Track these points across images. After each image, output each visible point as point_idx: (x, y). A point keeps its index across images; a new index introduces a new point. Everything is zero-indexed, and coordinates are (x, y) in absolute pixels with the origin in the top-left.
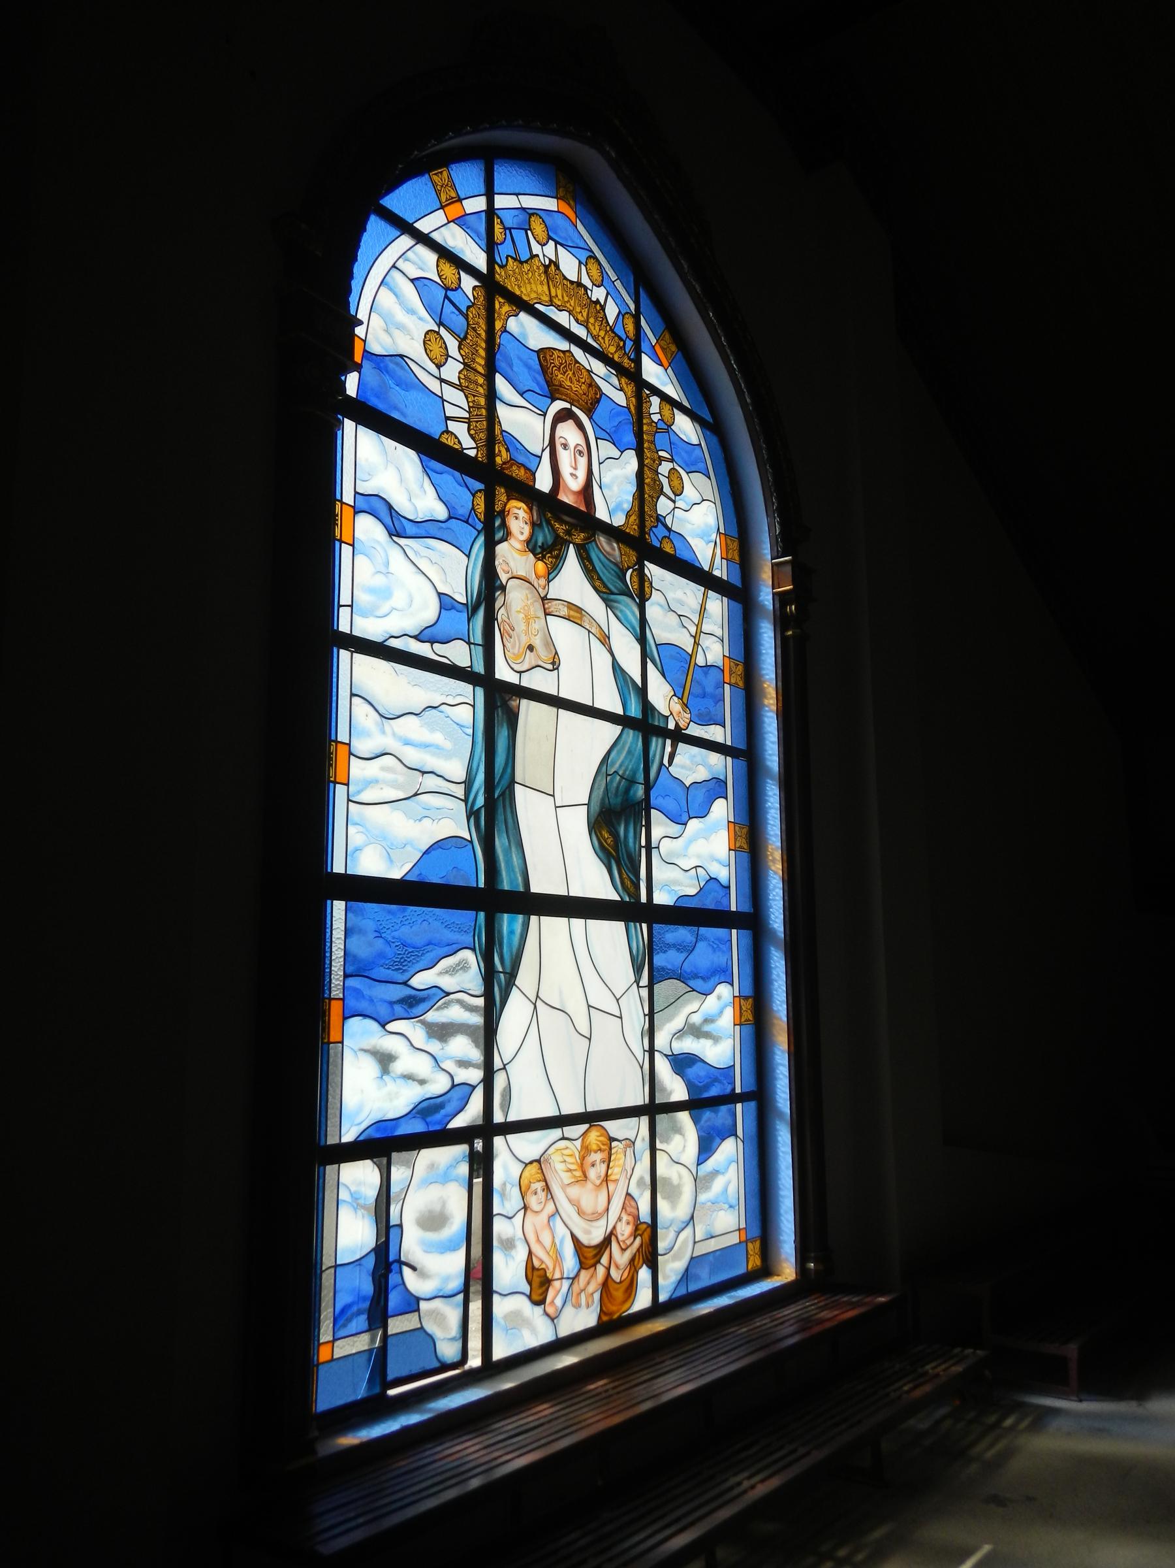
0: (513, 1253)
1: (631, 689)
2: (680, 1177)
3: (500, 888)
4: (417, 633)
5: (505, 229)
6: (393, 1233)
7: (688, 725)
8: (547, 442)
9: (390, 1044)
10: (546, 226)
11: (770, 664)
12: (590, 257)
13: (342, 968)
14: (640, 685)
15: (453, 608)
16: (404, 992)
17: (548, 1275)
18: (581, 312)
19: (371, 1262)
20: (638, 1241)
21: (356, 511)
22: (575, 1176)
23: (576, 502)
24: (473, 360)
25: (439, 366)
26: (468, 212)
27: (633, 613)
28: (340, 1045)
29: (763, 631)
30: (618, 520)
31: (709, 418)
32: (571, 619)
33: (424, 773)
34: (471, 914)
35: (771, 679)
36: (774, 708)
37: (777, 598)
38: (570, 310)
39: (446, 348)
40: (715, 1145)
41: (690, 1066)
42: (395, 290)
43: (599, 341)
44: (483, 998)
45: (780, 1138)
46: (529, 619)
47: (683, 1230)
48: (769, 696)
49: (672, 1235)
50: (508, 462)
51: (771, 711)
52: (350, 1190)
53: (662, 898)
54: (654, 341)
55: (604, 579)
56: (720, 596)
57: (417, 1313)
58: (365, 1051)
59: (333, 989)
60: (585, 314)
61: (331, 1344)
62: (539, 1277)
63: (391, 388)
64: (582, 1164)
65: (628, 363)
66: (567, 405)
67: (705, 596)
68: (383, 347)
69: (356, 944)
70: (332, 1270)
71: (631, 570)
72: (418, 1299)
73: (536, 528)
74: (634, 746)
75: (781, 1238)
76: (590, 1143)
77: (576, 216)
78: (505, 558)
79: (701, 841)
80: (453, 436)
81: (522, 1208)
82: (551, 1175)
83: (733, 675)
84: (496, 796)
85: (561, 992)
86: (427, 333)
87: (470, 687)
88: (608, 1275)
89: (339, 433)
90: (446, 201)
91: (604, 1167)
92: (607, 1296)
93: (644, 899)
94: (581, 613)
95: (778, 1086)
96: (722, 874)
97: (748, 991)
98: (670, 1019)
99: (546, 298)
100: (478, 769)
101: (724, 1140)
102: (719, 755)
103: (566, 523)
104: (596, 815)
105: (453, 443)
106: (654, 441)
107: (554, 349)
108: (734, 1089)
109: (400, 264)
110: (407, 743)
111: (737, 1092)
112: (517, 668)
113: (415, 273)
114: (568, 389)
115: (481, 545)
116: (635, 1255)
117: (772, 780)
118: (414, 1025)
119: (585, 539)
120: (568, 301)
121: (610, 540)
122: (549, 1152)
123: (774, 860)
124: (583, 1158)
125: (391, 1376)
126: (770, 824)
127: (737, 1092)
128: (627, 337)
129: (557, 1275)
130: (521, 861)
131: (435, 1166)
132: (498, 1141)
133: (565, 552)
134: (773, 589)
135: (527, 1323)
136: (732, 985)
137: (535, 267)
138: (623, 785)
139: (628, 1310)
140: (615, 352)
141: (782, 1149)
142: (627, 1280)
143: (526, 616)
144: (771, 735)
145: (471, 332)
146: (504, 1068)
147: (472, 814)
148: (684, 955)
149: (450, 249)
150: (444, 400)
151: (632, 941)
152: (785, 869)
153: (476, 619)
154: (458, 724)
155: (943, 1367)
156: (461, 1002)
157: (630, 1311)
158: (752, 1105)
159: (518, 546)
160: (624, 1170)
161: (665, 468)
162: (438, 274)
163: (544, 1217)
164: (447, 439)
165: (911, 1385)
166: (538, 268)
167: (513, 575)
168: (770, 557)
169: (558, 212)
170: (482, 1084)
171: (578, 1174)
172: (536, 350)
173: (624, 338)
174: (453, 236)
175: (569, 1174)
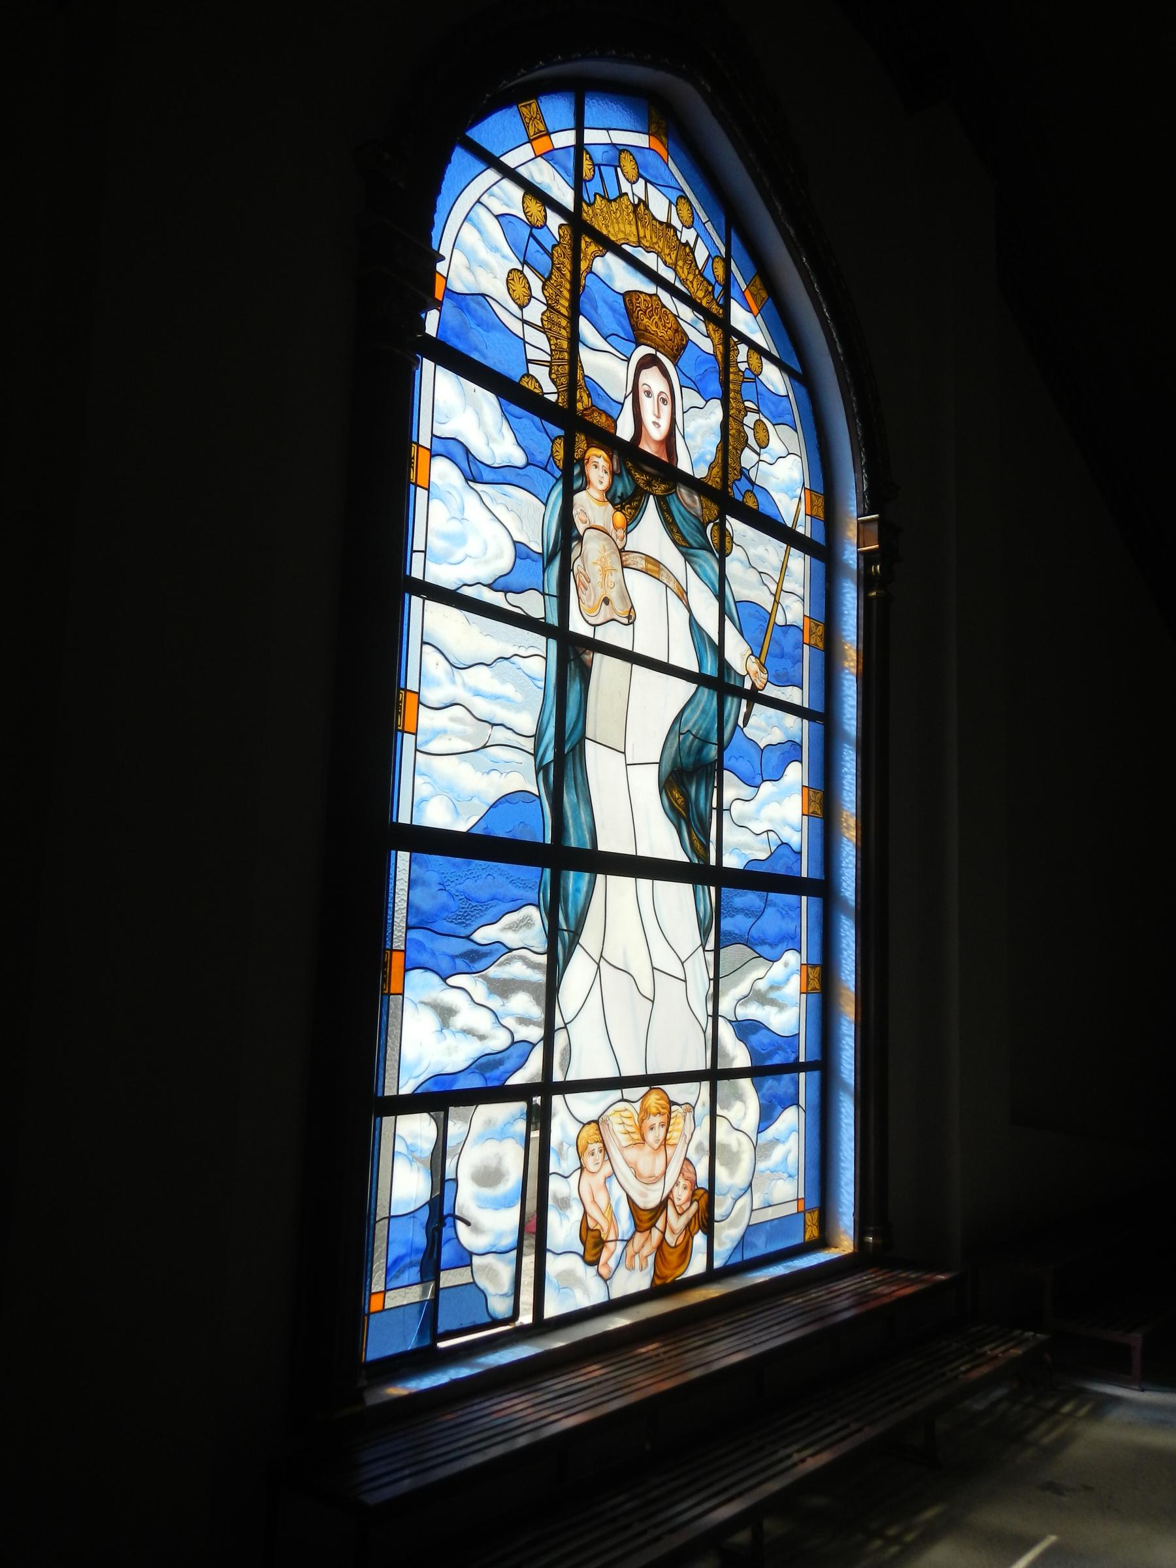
0: (568, 1212)
1: (708, 647)
2: (740, 1144)
3: (567, 845)
4: (491, 582)
5: (594, 165)
6: (448, 1187)
7: (765, 685)
8: (630, 389)
9: (451, 998)
10: (636, 163)
11: (852, 625)
12: (681, 197)
13: (405, 920)
14: (717, 643)
15: (528, 557)
16: (468, 946)
17: (602, 1236)
18: (669, 254)
19: (425, 1215)
20: (695, 1206)
21: (433, 455)
23: (657, 452)
24: (557, 302)
25: (521, 307)
26: (556, 147)
27: (713, 568)
28: (401, 997)
29: (846, 591)
30: (701, 472)
31: (797, 368)
32: (649, 572)
33: (493, 725)
34: (534, 871)
35: (853, 641)
36: (854, 671)
37: (862, 557)
38: (658, 252)
39: (530, 288)
40: (776, 1114)
41: (754, 1033)
42: (479, 226)
43: (687, 284)
44: (545, 956)
45: (843, 1110)
46: (605, 571)
47: (740, 1197)
48: (849, 659)
49: (729, 1201)
50: (589, 408)
51: (851, 673)
52: (406, 1142)
53: (730, 861)
54: (744, 287)
55: (684, 532)
56: (803, 554)
57: (469, 1268)
59: (394, 940)
60: (673, 257)
61: (382, 1294)
62: (593, 1237)
63: (471, 328)
64: (641, 1127)
65: (717, 309)
66: (652, 351)
67: (787, 554)
68: (465, 286)
69: (419, 895)
70: (386, 1221)
71: (712, 524)
72: (471, 1254)
73: (616, 477)
74: (709, 704)
75: (841, 1210)
76: (649, 1106)
77: (668, 154)
78: (582, 506)
79: (775, 805)
80: (534, 380)
81: (578, 1169)
82: (608, 1135)
83: (812, 636)
84: (566, 752)
85: (625, 954)
86: (510, 272)
87: (544, 639)
88: (663, 1240)
89: (418, 373)
90: (534, 134)
91: (663, 1130)
92: (662, 1262)
93: (713, 862)
94: (659, 567)
95: (843, 1056)
96: (795, 839)
97: (816, 959)
98: (735, 984)
99: (633, 239)
100: (548, 723)
101: (785, 1109)
103: (647, 473)
104: (667, 775)
105: (533, 387)
106: (741, 391)
107: (641, 292)
108: (798, 1058)
109: (484, 199)
110: (477, 694)
111: (800, 1061)
112: (593, 621)
113: (499, 209)
114: (653, 334)
115: (559, 494)
116: (691, 1220)
117: (848, 745)
118: (475, 980)
119: (666, 490)
120: (657, 243)
121: (692, 493)
122: (608, 1113)
123: (848, 828)
124: (642, 1121)
125: (441, 1329)
126: (845, 790)
127: (800, 1061)
128: (717, 281)
129: (612, 1237)
130: (589, 819)
131: (492, 1122)
132: (557, 1100)
133: (645, 504)
134: (858, 548)
135: (579, 1282)
136: (800, 952)
137: (624, 206)
138: (696, 745)
140: (704, 297)
141: (845, 1121)
142: (683, 1244)
143: (602, 568)
144: (850, 698)
145: (555, 273)
146: (565, 1027)
147: (541, 768)
148: (751, 920)
149: (535, 184)
150: (525, 342)
151: (700, 904)
152: (859, 837)
153: (551, 570)
154: (529, 677)
155: (1003, 1348)
156: (523, 959)
157: (684, 1276)
158: (816, 1075)
159: (597, 495)
160: (683, 1134)
161: (750, 420)
162: (524, 211)
163: (600, 1177)
164: (528, 383)
165: (968, 1366)
166: (627, 207)
167: (591, 525)
168: (855, 514)
169: (649, 148)
170: (542, 1042)
171: (637, 1136)
172: (622, 292)
173: (713, 283)
174: (541, 172)
175: (627, 1136)
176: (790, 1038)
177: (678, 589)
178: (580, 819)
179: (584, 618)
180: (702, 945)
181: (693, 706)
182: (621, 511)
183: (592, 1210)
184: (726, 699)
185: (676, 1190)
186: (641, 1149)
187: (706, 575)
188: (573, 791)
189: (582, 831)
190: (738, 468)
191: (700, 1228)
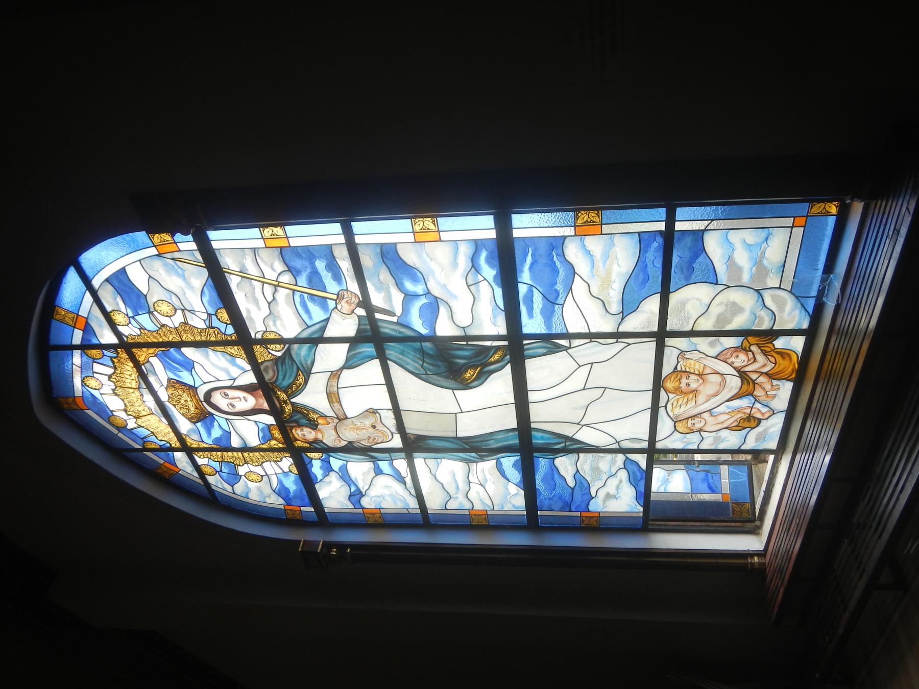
17: (745, 417)
20: (754, 348)
22: (692, 398)
33: (470, 482)
44: (580, 454)
64: (686, 393)
74: (396, 349)
76: (673, 387)
84: (468, 447)
85: (576, 409)
88: (766, 374)
91: (693, 377)
93: (505, 343)
96: (465, 251)
100: (457, 456)
104: (457, 383)
108: (660, 232)
112: (390, 437)
116: (762, 350)
118: (593, 485)
124: (682, 392)
127: (663, 229)
130: (501, 433)
132: (659, 445)
146: (618, 442)
147: (482, 459)
151: (537, 352)
156: (581, 465)
160: (698, 361)
171: (691, 396)
175: (689, 402)
176: (642, 246)
177: (333, 378)
178: (502, 438)
179: (388, 429)
180: (566, 350)
181: (403, 363)
182: (317, 421)
183: (726, 425)
184: (385, 333)
185: (736, 365)
186: (700, 392)
187: (309, 355)
189: (508, 437)
190: (211, 331)
191: (771, 343)
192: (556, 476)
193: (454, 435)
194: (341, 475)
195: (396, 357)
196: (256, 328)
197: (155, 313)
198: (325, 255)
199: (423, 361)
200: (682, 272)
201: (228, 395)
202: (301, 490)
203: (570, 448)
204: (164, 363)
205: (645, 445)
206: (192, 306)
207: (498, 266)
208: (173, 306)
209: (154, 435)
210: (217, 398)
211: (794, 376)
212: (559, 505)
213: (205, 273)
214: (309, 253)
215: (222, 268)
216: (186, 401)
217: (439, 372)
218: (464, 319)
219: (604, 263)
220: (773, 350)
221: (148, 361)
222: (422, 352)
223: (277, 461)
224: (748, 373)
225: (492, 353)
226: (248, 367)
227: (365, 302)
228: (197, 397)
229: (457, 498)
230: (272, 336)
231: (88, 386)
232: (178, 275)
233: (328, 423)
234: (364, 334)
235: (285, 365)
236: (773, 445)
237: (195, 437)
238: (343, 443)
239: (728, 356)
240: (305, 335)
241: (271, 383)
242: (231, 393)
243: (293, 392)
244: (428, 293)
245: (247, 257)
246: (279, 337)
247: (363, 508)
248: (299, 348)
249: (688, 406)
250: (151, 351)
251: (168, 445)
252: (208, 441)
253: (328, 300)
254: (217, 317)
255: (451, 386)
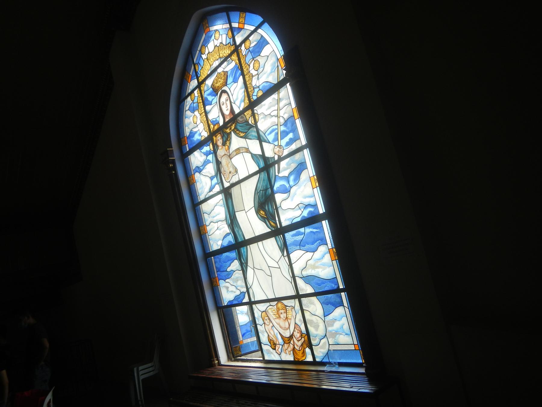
1: (259, 158)
33: (217, 222)
44: (241, 271)
53: (284, 224)
58: (224, 286)
84: (232, 218)
88: (294, 347)
91: (285, 314)
93: (279, 227)
96: (311, 201)
102: (299, 153)
103: (229, 127)
112: (228, 181)
116: (303, 343)
124: (278, 311)
127: (340, 288)
130: (241, 233)
132: (254, 306)
139: (304, 360)
146: (251, 287)
147: (229, 226)
156: (237, 272)
160: (292, 316)
171: (277, 316)
176: (332, 280)
177: (246, 150)
180: (282, 255)
181: (260, 181)
183: (270, 334)
185: (295, 333)
186: (280, 320)
188: (236, 227)
189: (240, 236)
190: (252, 89)
192: (230, 262)
193: (236, 211)
194: (206, 161)
195: (262, 178)
196: (258, 110)
197: (254, 61)
198: (295, 137)
199: (263, 190)
200: (325, 300)
201: (227, 101)
202: (195, 143)
203: (243, 266)
204: (234, 68)
205: (253, 300)
206: (260, 78)
207: (309, 217)
208: (259, 69)
209: (202, 68)
210: (224, 96)
211: (296, 360)
212: (218, 266)
213: (276, 82)
214: (294, 130)
215: (279, 90)
216: (220, 82)
217: (260, 199)
218: (285, 205)
219: (321, 264)
220: (304, 348)
221: (232, 61)
222: (266, 190)
223: (204, 129)
224: (292, 339)
225: (273, 221)
226: (241, 109)
227: (281, 159)
228: (223, 86)
229: (209, 218)
230: (257, 118)
231: (215, 33)
232: (272, 69)
233: (227, 151)
234: (267, 160)
235: (247, 126)
236: (267, 358)
237: (206, 88)
238: (220, 159)
239: (297, 329)
240: (261, 133)
241: (237, 121)
242: (228, 102)
243: (236, 131)
244: (291, 187)
245: (287, 101)
246: (257, 121)
247: (194, 174)
248: (254, 131)
249: (273, 316)
250: (237, 61)
251: (199, 76)
252: (205, 95)
253: (277, 141)
254: (259, 91)
255: (256, 205)
